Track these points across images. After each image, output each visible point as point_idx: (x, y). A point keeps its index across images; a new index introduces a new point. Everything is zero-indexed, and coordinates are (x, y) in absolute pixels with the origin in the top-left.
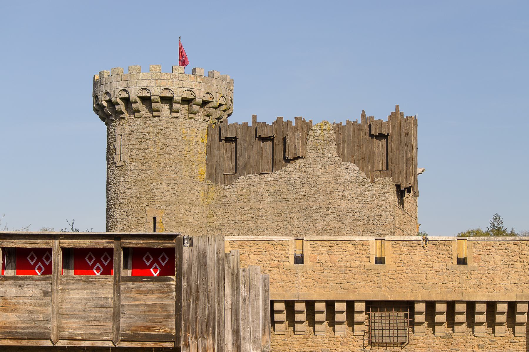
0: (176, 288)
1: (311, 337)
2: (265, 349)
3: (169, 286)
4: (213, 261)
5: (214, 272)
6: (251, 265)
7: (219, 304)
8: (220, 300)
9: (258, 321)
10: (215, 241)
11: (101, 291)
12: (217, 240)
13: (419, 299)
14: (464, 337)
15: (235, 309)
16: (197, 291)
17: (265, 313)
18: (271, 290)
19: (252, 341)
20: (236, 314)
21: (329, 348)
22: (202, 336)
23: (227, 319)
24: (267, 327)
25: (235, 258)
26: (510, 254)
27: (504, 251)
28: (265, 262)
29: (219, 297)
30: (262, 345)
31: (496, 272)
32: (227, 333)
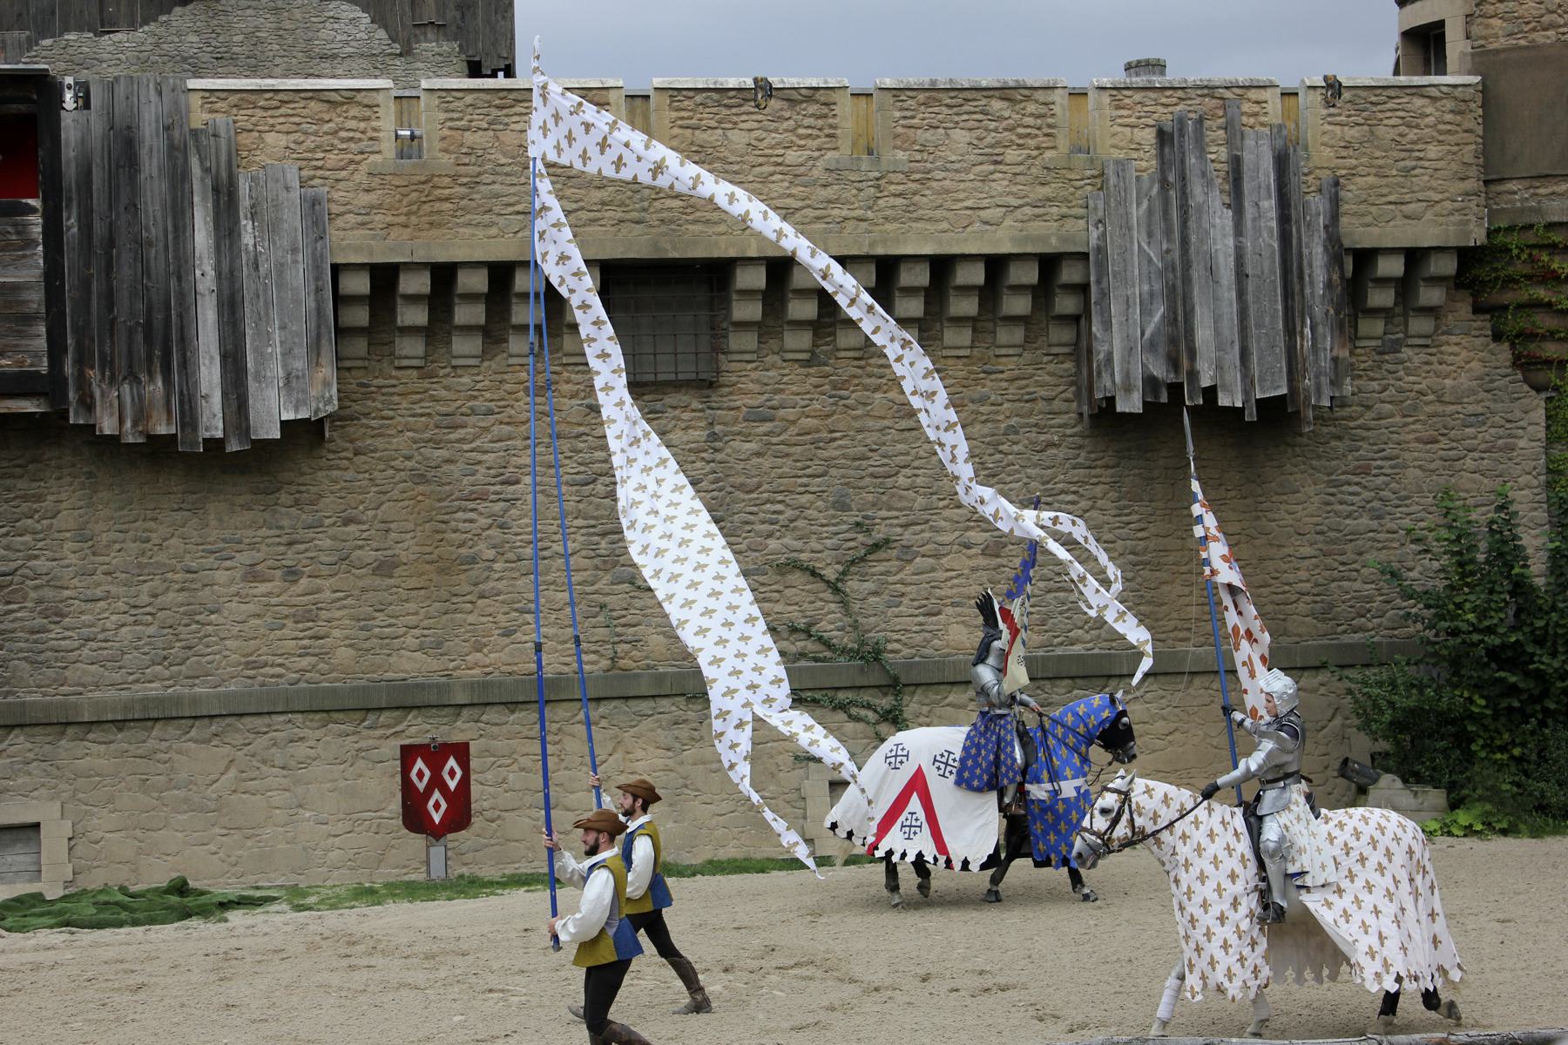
0: (44, 233)
1: (442, 372)
2: (321, 405)
3: (22, 229)
4: (155, 154)
5: (160, 185)
6: (270, 162)
7: (179, 278)
8: (182, 264)
9: (298, 326)
10: (160, 93)
12: (164, 89)
13: (753, 253)
14: (862, 363)
15: (226, 292)
16: (111, 242)
17: (317, 301)
18: (334, 234)
19: (281, 385)
20: (231, 308)
21: (493, 403)
22: (133, 377)
23: (205, 322)
24: (324, 341)
25: (223, 142)
26: (993, 125)
27: (975, 116)
28: (310, 155)
29: (177, 258)
30: (313, 393)
31: (958, 176)
32: (207, 362)
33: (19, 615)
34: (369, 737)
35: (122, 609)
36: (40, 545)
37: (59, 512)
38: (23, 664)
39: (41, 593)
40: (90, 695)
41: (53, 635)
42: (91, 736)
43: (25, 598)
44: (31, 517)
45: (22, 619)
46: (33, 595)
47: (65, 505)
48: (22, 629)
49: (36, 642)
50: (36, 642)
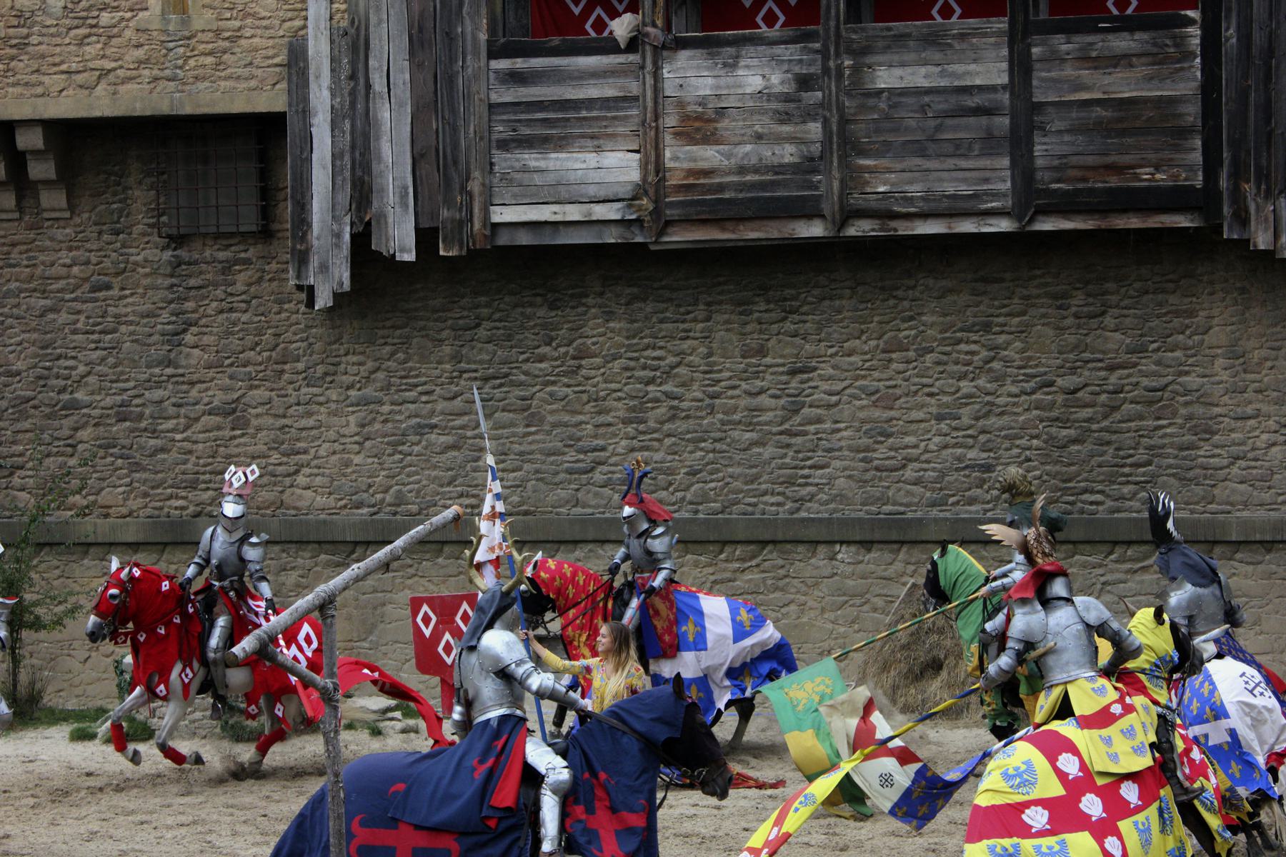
0: (1202, 44)
3: (1180, 41)
11: (972, 67)
33: (1168, 430)
34: (1118, 571)
35: (1273, 428)
36: (1191, 361)
37: (1210, 328)
38: (1172, 480)
39: (1190, 409)
40: (1238, 514)
41: (1201, 453)
42: (1238, 556)
43: (1174, 414)
44: (1183, 333)
45: (1171, 435)
46: (1183, 411)
47: (1216, 321)
48: (1172, 445)
49: (1184, 458)
50: (1184, 458)
